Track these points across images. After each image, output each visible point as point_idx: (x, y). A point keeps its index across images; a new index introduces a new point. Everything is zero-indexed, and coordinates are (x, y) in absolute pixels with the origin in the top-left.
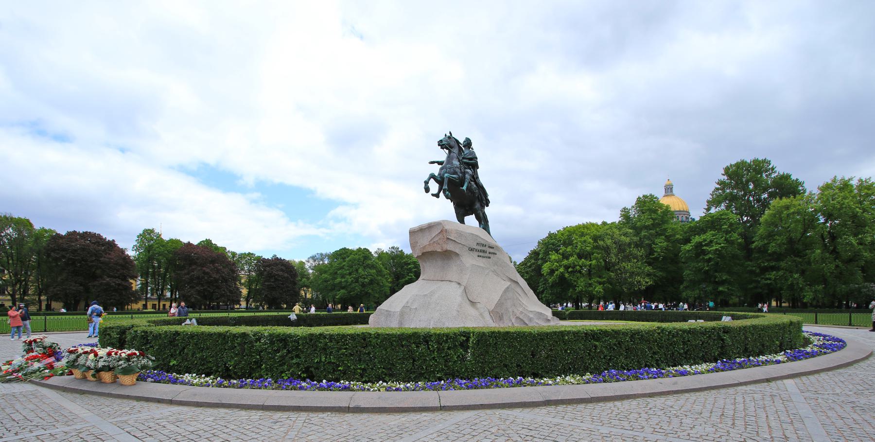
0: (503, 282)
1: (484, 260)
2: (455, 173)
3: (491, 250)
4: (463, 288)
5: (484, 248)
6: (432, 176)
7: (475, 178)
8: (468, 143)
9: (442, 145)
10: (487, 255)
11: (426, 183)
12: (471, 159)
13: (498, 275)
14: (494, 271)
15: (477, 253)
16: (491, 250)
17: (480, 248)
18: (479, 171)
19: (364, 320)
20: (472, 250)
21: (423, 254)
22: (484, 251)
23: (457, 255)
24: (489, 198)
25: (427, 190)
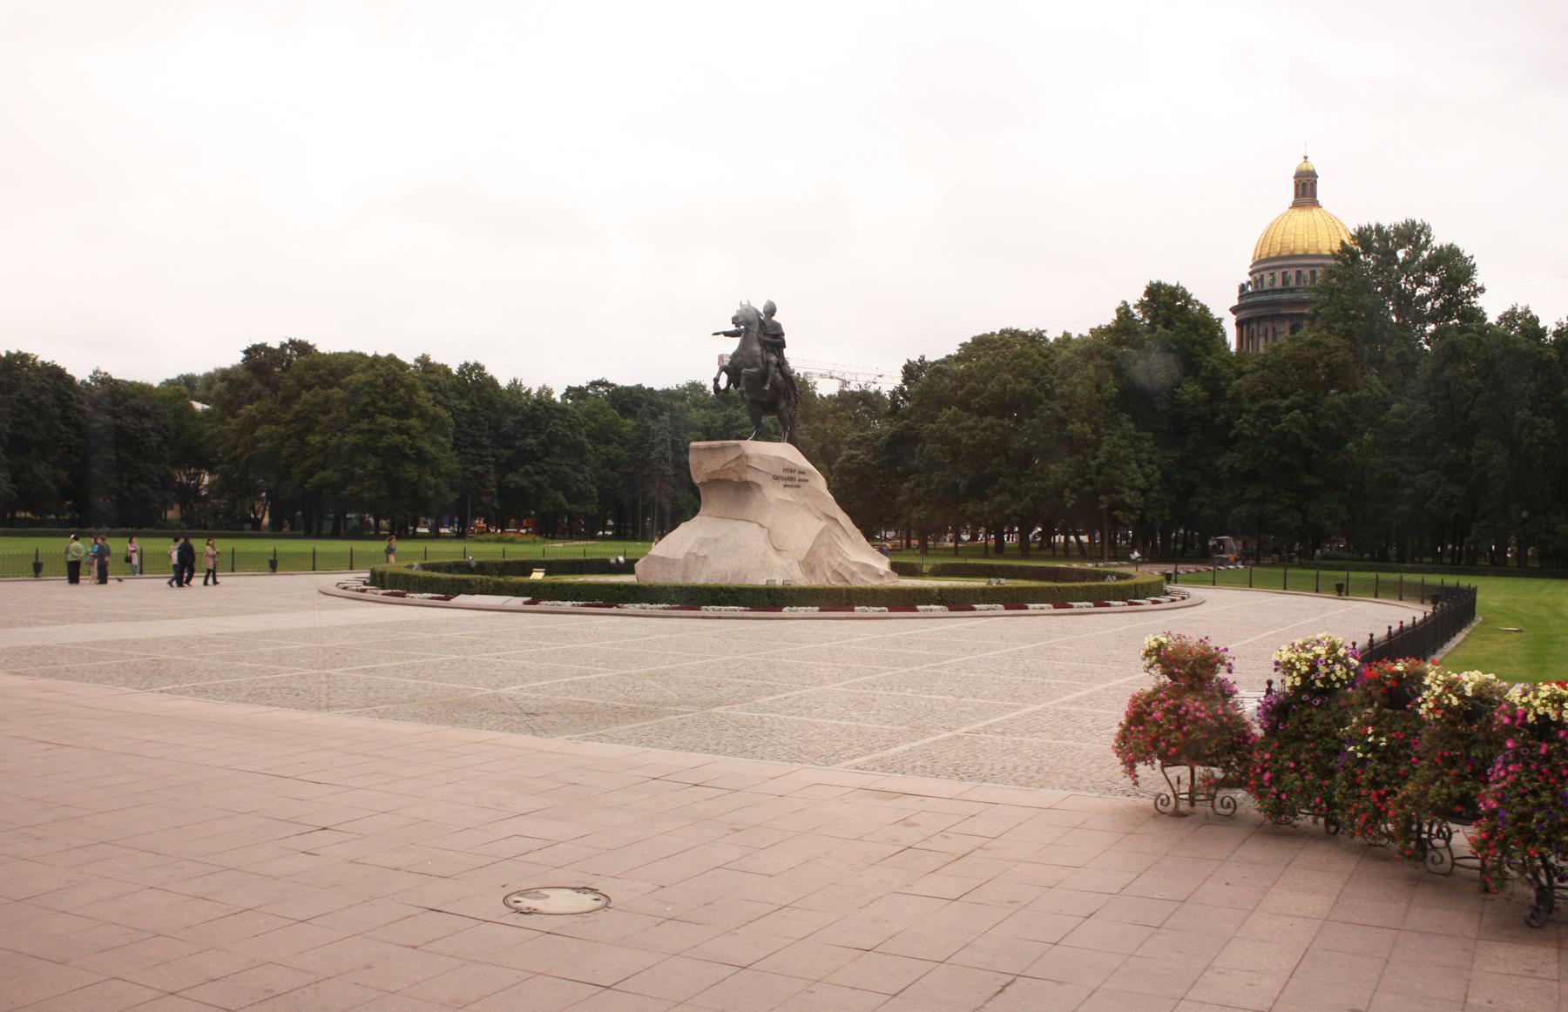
0: (816, 522)
2: (755, 365)
7: (782, 364)
8: (771, 310)
13: (809, 510)
14: (805, 506)
17: (786, 475)
18: (787, 353)
19: (628, 567)
20: (776, 478)
21: (710, 481)
22: (792, 479)
23: (759, 486)
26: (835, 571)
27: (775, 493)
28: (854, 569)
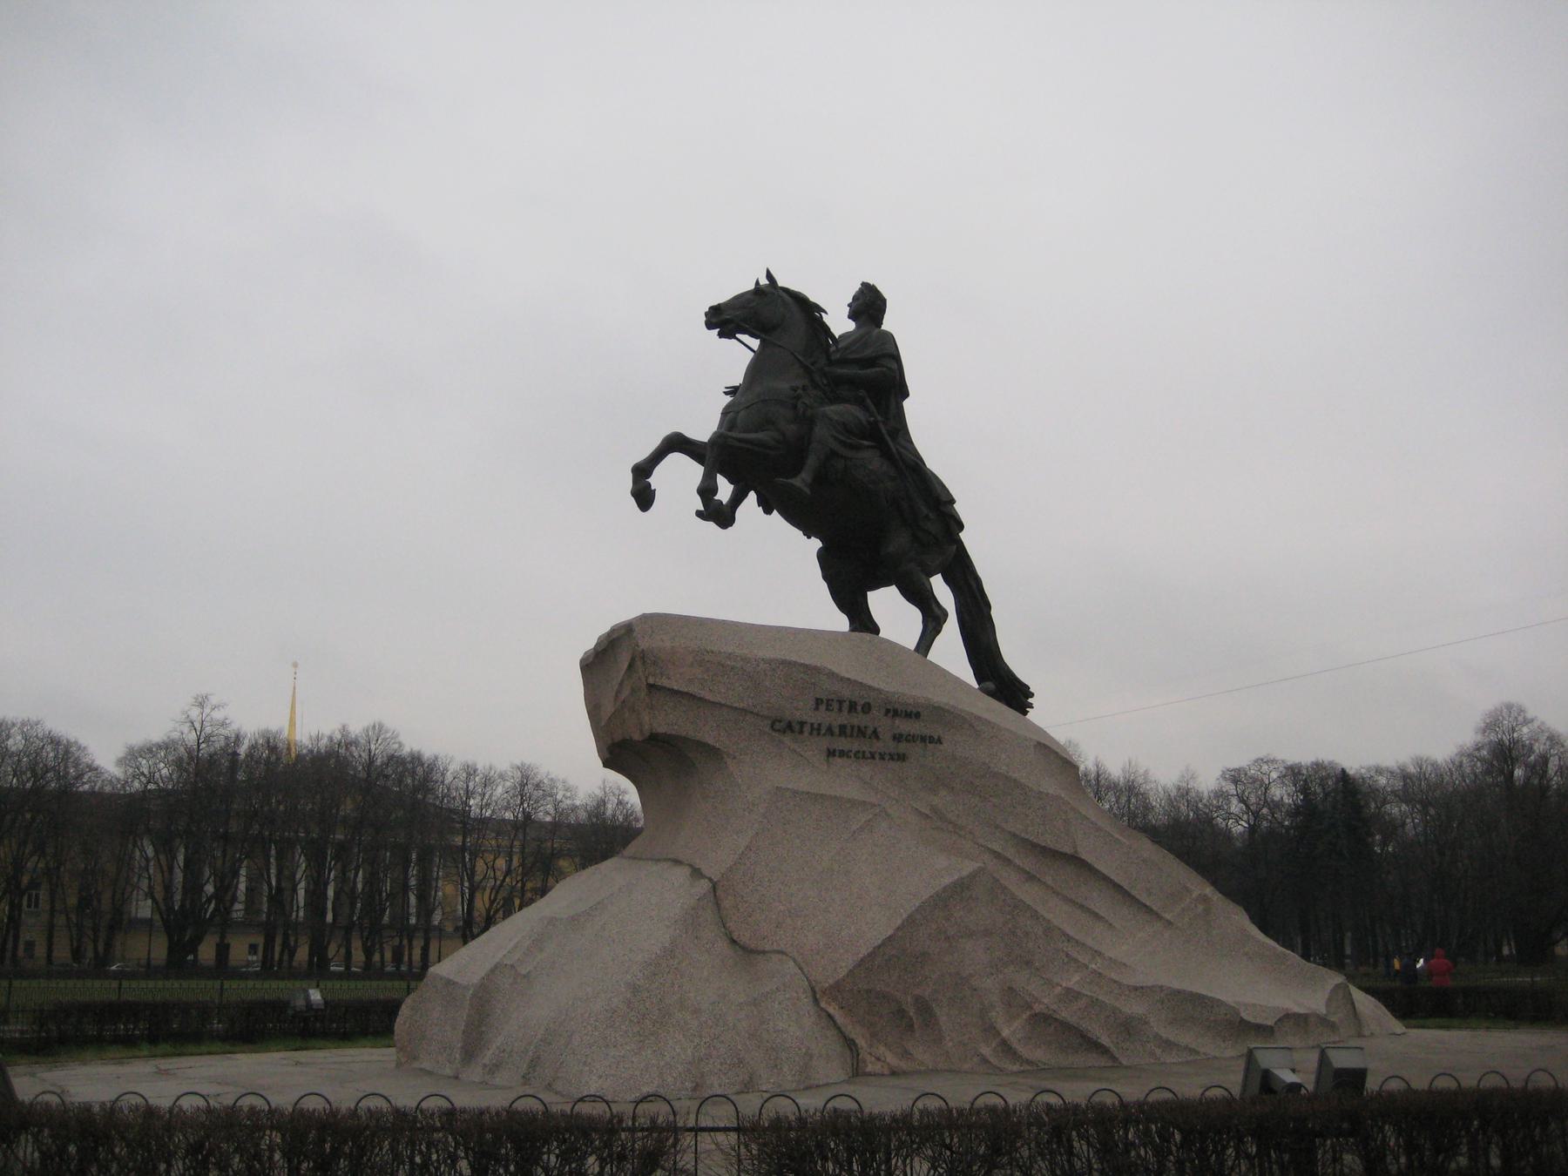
1: (866, 769)
3: (905, 726)
4: (704, 886)
5: (858, 720)
6: (676, 443)
9: (724, 320)
10: (886, 744)
11: (642, 472)
12: (871, 362)
15: (824, 742)
16: (905, 726)
20: (790, 727)
22: (861, 732)
23: (713, 753)
24: (959, 507)
25: (644, 497)
26: (1042, 1021)
27: (768, 774)
28: (1134, 1008)
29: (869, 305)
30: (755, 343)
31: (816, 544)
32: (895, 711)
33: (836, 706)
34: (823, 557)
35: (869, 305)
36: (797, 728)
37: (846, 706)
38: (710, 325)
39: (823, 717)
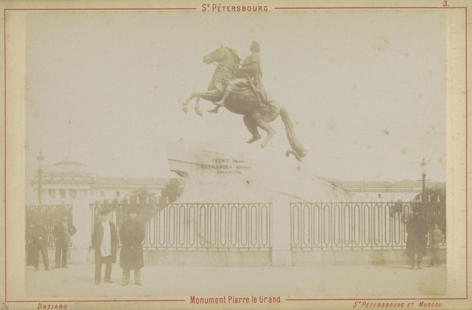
5: (226, 164)
12: (250, 64)
25: (185, 110)
29: (255, 48)
30: (217, 64)
31: (242, 116)
32: (236, 161)
33: (218, 161)
34: (245, 118)
35: (255, 48)
36: (208, 167)
37: (221, 161)
38: (204, 62)
39: (214, 164)
